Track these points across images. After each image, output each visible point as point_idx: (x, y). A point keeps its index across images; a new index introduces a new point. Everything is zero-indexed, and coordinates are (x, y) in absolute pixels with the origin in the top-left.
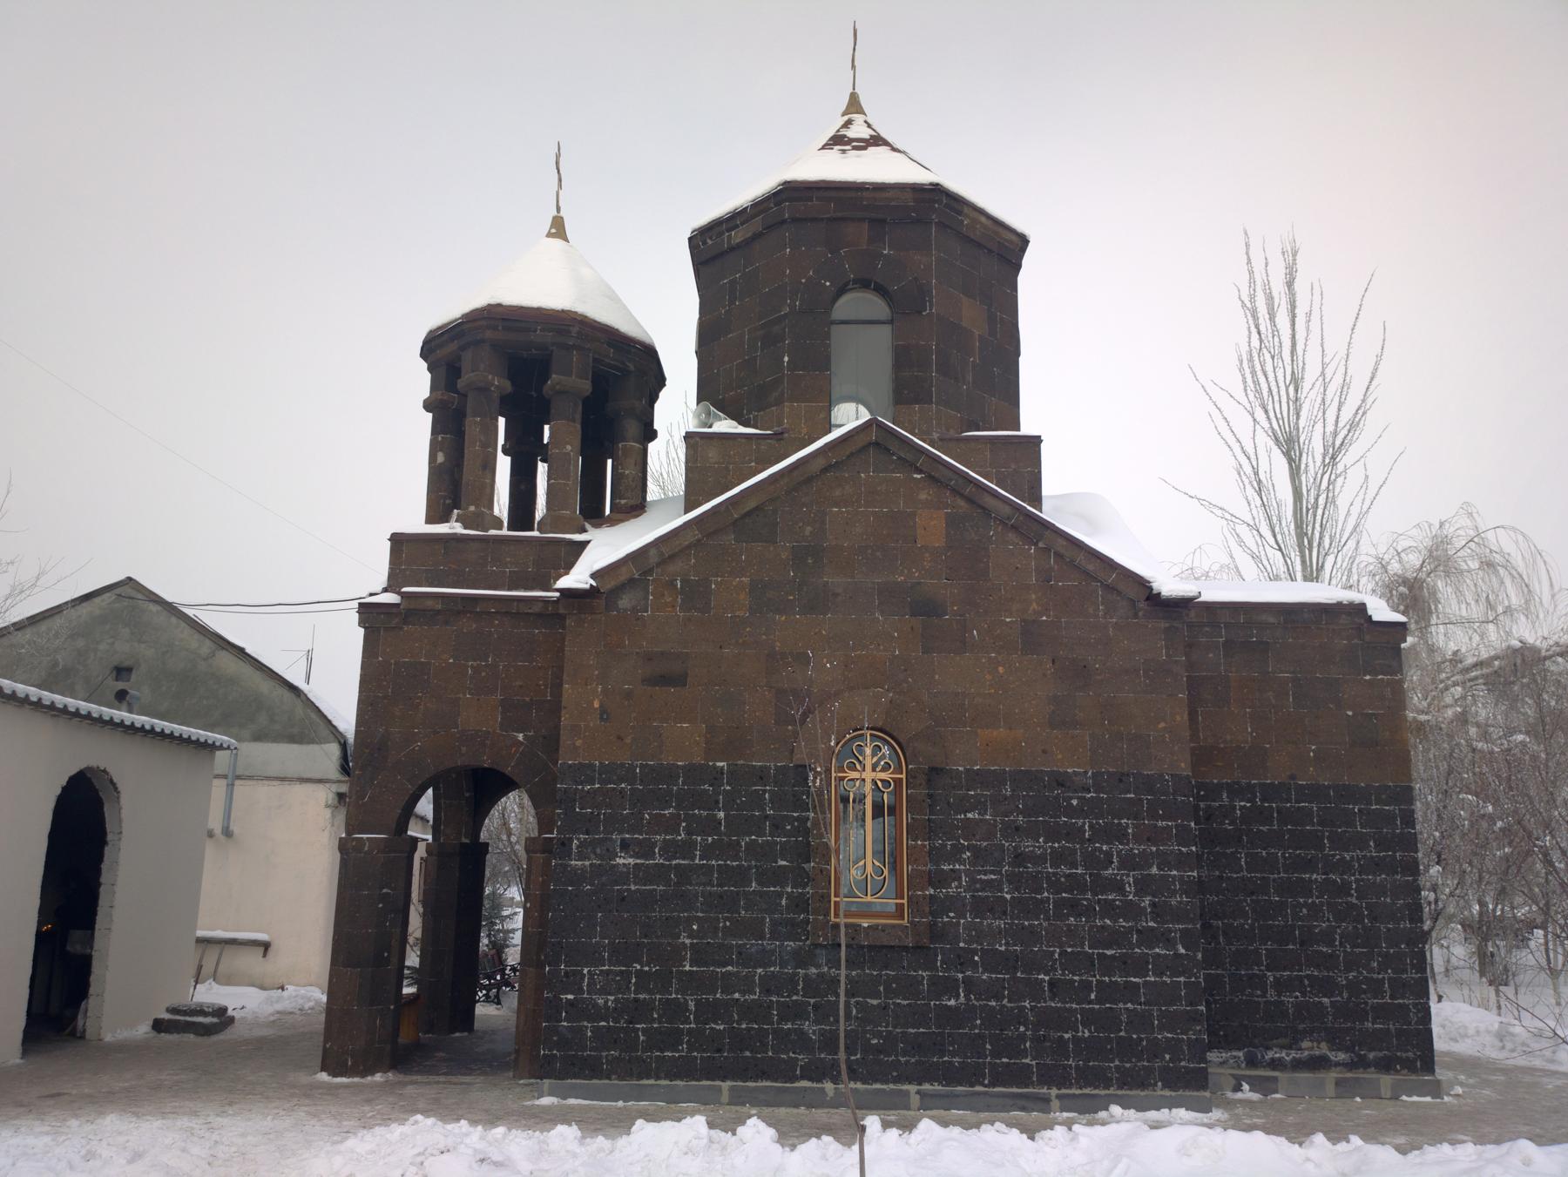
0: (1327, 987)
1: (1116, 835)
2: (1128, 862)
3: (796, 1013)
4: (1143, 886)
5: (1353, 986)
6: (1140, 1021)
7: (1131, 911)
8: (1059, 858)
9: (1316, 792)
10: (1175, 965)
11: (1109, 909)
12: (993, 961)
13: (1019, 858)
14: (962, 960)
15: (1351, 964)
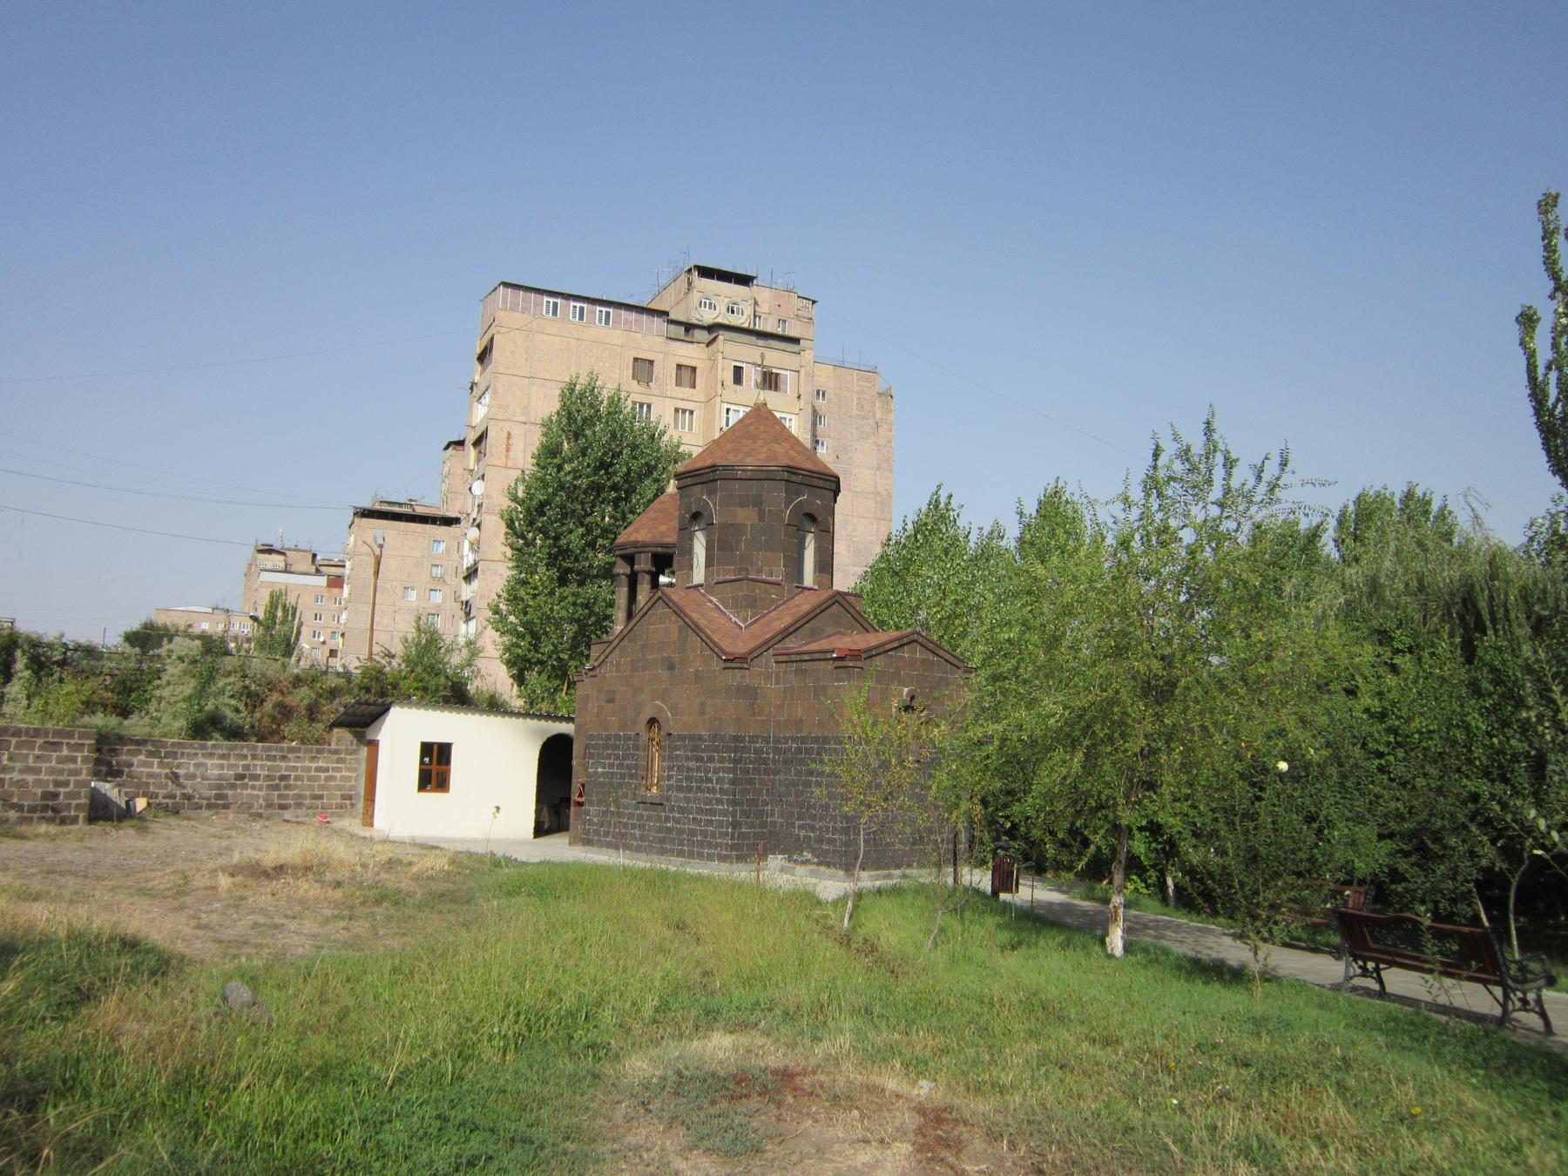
0: (813, 829)
1: (711, 759)
2: (716, 771)
3: (634, 827)
4: (718, 779)
5: (821, 828)
6: (713, 835)
7: (713, 791)
8: (698, 769)
9: (816, 740)
10: (723, 813)
11: (710, 790)
12: (682, 810)
13: (689, 769)
14: (672, 810)
15: (821, 819)
